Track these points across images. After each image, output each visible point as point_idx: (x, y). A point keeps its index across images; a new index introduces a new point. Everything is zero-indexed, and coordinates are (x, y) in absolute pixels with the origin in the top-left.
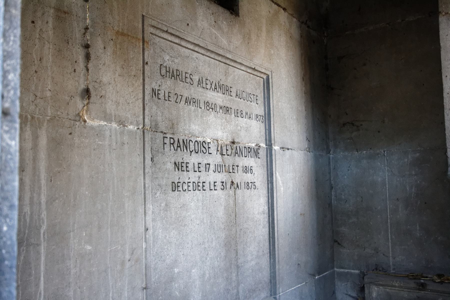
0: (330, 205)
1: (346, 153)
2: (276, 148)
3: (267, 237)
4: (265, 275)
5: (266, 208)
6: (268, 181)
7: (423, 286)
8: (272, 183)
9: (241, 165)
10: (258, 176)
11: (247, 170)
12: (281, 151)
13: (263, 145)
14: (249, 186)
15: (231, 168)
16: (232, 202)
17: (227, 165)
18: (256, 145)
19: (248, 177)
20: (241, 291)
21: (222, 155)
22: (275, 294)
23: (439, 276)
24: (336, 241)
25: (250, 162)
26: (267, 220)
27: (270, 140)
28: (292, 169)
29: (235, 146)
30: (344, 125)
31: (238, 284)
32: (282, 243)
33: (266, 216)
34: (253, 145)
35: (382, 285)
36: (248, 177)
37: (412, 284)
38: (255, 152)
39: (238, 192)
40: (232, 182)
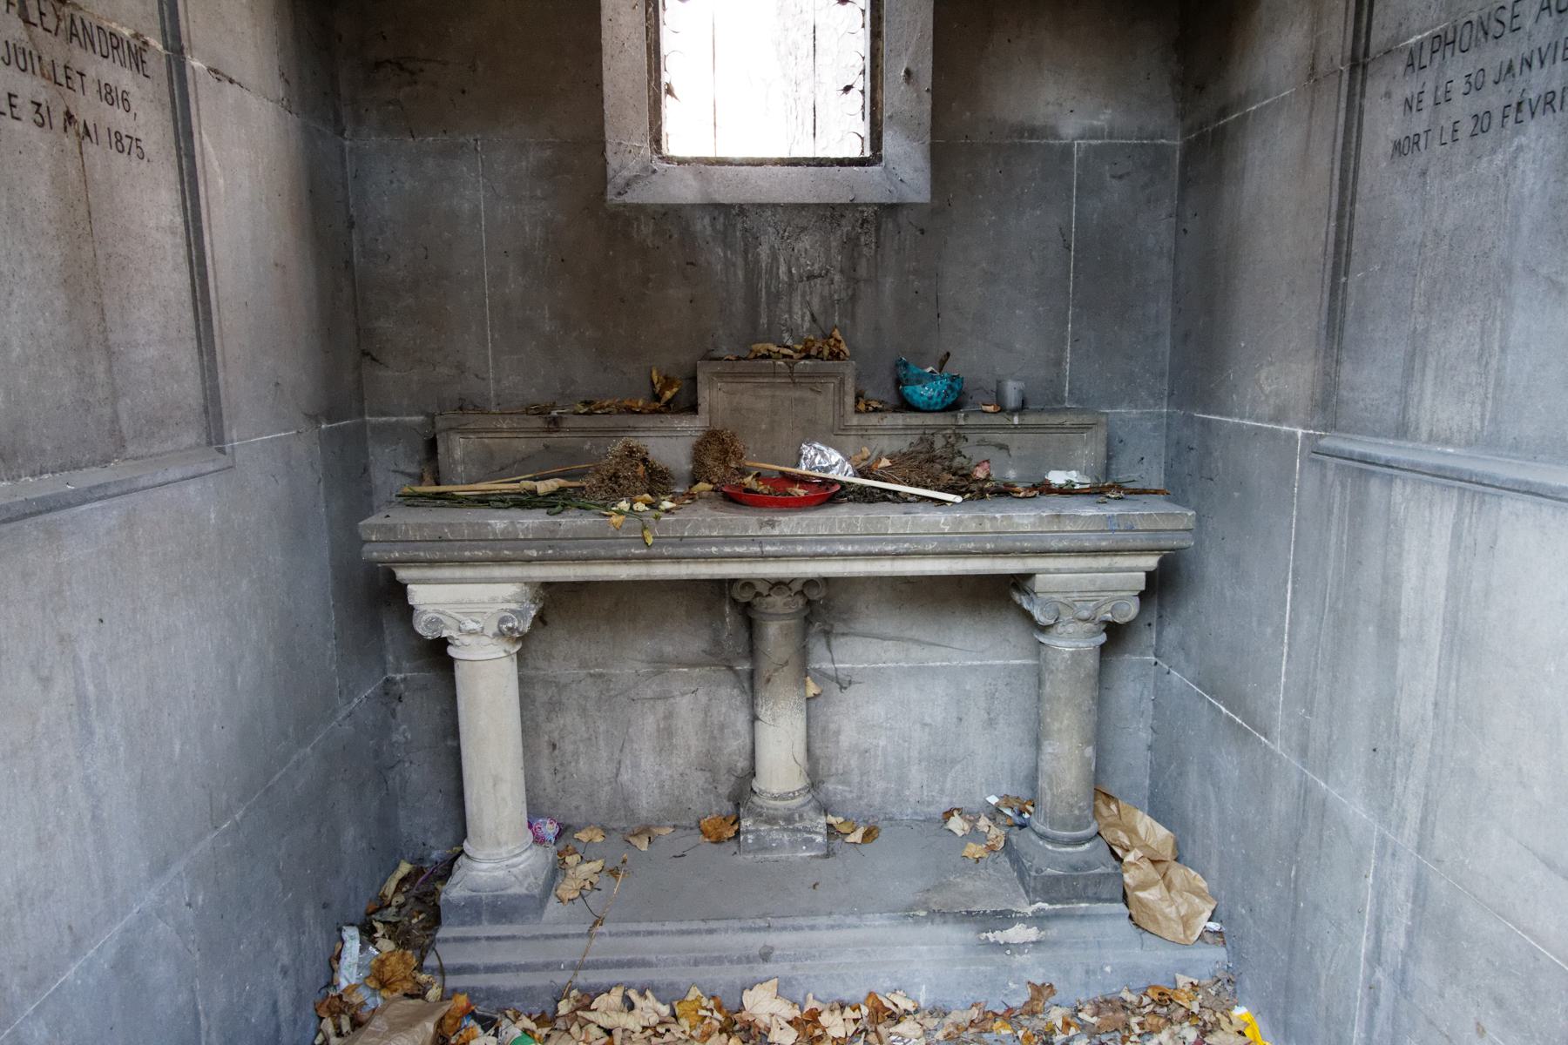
0: (348, 264)
1: (386, 140)
2: (196, 63)
3: (186, 296)
4: (189, 389)
5: (179, 220)
6: (179, 148)
7: (555, 424)
8: (192, 158)
9: (91, 73)
10: (147, 120)
11: (109, 95)
12: (211, 79)
13: (156, 43)
14: (118, 140)
15: (60, 72)
16: (73, 174)
17: (46, 59)
18: (136, 36)
19: (116, 117)
20: (124, 417)
21: (27, 21)
22: (220, 439)
23: (586, 403)
24: (365, 353)
25: (124, 78)
26: (183, 251)
27: (177, 37)
28: (247, 140)
29: (67, 10)
30: (378, 65)
31: (115, 396)
32: (230, 320)
33: (181, 240)
34: (126, 32)
35: (474, 431)
36: (116, 117)
37: (538, 422)
38: (137, 56)
39: (90, 148)
40: (69, 117)
